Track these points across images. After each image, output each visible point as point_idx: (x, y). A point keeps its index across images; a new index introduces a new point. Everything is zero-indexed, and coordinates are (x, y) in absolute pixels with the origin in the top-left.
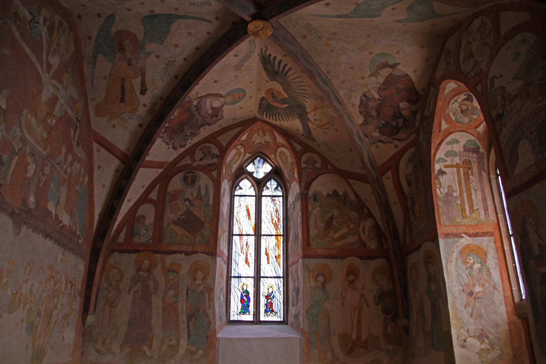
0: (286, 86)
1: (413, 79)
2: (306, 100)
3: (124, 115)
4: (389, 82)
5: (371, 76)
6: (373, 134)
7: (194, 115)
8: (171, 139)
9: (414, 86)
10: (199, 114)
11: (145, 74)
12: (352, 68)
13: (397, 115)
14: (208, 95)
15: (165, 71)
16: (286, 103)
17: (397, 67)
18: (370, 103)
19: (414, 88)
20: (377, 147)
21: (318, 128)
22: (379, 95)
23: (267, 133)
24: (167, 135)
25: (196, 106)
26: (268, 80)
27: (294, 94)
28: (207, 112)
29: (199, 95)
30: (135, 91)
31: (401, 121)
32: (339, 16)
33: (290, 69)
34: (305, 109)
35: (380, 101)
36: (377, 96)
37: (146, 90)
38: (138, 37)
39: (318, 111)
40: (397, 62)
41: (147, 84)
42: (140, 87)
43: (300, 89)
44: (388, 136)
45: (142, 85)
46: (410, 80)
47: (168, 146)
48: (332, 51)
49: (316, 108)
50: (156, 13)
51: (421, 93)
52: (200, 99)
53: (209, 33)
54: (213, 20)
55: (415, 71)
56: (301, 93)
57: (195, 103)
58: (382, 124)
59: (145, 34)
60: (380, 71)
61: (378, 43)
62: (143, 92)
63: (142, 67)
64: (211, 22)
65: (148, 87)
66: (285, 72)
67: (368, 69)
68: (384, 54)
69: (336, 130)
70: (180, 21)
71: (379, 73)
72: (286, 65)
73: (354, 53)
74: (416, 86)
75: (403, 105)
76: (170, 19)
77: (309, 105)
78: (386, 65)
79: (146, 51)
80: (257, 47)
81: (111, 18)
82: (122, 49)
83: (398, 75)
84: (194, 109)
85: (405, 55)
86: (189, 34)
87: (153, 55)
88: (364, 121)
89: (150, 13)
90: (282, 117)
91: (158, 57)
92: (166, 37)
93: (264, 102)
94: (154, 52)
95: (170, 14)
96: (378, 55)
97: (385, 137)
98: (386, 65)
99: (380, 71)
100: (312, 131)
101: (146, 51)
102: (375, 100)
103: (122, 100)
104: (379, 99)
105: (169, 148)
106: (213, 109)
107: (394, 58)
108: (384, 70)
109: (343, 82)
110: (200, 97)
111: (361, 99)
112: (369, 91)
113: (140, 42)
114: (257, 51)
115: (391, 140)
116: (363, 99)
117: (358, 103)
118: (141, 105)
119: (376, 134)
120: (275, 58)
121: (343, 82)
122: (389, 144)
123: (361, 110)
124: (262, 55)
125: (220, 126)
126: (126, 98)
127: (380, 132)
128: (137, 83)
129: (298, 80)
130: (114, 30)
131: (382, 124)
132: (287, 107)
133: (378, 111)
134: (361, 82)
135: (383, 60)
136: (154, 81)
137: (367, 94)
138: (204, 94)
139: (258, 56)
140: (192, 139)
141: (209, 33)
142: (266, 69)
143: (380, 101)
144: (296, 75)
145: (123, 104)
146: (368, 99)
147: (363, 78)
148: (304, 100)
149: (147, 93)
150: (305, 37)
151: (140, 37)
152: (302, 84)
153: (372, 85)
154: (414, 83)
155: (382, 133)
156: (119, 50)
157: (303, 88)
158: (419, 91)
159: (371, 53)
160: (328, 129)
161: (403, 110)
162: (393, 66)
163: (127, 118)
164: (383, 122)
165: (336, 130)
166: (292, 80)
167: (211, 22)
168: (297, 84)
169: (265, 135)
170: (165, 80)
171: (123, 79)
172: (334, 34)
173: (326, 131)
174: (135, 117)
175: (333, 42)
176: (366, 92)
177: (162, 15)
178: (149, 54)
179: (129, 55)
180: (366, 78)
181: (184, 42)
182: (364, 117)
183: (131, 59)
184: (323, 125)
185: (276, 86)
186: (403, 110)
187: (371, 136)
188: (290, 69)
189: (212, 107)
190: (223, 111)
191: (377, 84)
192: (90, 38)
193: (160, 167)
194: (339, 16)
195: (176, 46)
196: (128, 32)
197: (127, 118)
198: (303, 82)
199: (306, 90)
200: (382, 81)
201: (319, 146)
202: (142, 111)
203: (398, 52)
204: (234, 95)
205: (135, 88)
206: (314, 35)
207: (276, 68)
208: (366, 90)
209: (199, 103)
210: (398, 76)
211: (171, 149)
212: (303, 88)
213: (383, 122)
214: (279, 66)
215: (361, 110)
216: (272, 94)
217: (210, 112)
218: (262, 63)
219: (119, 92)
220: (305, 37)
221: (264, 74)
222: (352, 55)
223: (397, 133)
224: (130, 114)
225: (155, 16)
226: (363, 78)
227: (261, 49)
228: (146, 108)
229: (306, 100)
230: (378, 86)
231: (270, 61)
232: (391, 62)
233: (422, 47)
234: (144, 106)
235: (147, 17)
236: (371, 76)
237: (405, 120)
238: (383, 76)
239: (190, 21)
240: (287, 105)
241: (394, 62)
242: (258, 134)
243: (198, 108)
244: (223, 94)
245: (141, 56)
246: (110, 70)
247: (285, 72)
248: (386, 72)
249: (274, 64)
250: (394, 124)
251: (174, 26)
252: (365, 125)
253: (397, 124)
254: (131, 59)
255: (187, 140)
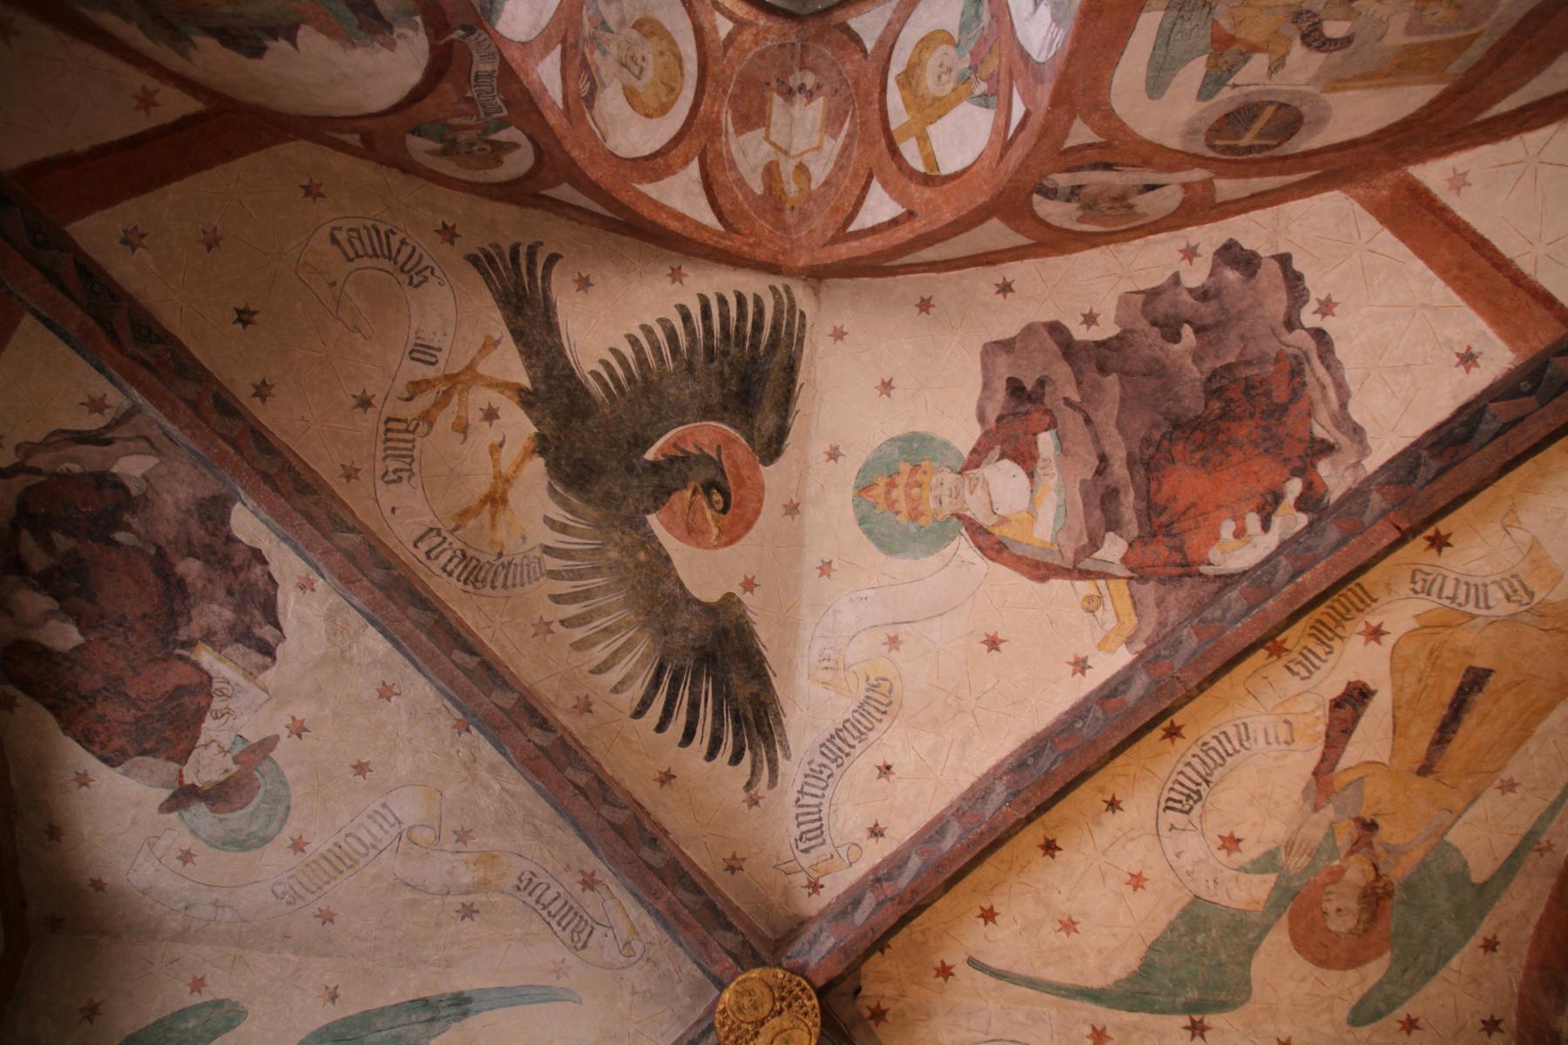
0: (656, 592)
1: (77, 747)
2: (553, 539)
3: (1501, 608)
4: (174, 724)
5: (267, 744)
6: (150, 462)
7: (1131, 462)
8: (1296, 368)
9: (58, 716)
10: (1103, 459)
11: (1315, 773)
12: (361, 768)
13: (70, 586)
14: (1041, 570)
15: (1218, 772)
16: (655, 466)
17: (165, 794)
18: (228, 614)
19: (50, 708)
20: (97, 406)
21: (471, 367)
22: (197, 666)
23: (757, 187)
24: (1310, 414)
25: (1113, 524)
26: (746, 598)
27: (614, 554)
28: (1063, 449)
29: (1085, 587)
30: (1396, 707)
31: (39, 560)
32: (461, 1004)
33: (639, 713)
34: (554, 467)
35: (183, 635)
36: (206, 657)
37: (1337, 704)
38: (1287, 939)
39: (481, 484)
40: (174, 815)
41: (1322, 728)
42: (1363, 721)
43: (587, 595)
44: (67, 477)
45: (1347, 732)
46: (86, 741)
47: (1329, 325)
48: (462, 836)
49: (496, 500)
50: (1184, 1020)
51: (11, 690)
52: (1086, 564)
53: (989, 915)
54: (961, 969)
55: (83, 780)
56: (579, 575)
57: (1113, 549)
58: (128, 528)
59: (1252, 949)
60: (234, 768)
61: (279, 890)
62: (1356, 697)
63: (1316, 808)
64: (972, 962)
65: (1323, 714)
66: (666, 679)
67: (289, 774)
68: (240, 843)
69: (365, 403)
70: (1096, 982)
71: (236, 760)
72: (661, 727)
73: (368, 839)
74: (49, 716)
75: (66, 636)
76: (1134, 994)
77: (536, 509)
78: (220, 795)
79: (1272, 878)
80: (793, 795)
81: (1363, 1014)
82: (1375, 898)
83: (149, 760)
84: (1128, 505)
85: (151, 846)
86: (1069, 926)
87: (1251, 851)
88: (225, 520)
89: (1211, 1019)
90: (675, 350)
91: (1231, 843)
92: (1172, 927)
93: (768, 422)
94: (1242, 869)
95: (1130, 1010)
96: (265, 840)
97: (76, 468)
98: (220, 795)
99: (234, 768)
100: (500, 330)
101: (1272, 878)
102: (208, 637)
103: (1475, 680)
104: (190, 644)
105: (1326, 307)
106: (1026, 458)
107: (194, 832)
108: (216, 777)
109: (386, 692)
110: (1086, 575)
111: (277, 626)
112: (250, 675)
113: (1284, 919)
114: (792, 770)
115: (41, 460)
116: (267, 632)
117: (290, 603)
118: (1388, 641)
119: (132, 467)
120: (711, 754)
121: (386, 692)
122: (38, 436)
123: (258, 570)
124: (770, 747)
125: (1005, 288)
126: (1451, 684)
127: (118, 484)
128: (1371, 739)
129: (600, 653)
130: (1375, 970)
131: (128, 528)
132: (648, 443)
133: (175, 590)
134: (303, 711)
135: (236, 819)
136: (1283, 735)
137: (256, 658)
138: (1058, 585)
139: (790, 736)
140: (1176, 279)
141: (989, 915)
142: (755, 666)
143: (183, 635)
144: (614, 676)
145: (1480, 662)
146: (243, 635)
147: (299, 729)
148: (563, 529)
149: (1338, 690)
150: (589, 883)
151: (1278, 939)
152: (579, 633)
153: (244, 707)
154: (67, 728)
155: (106, 482)
156: (1389, 894)
157: (573, 610)
158: (22, 699)
159: (298, 846)
160: (417, 388)
161: (48, 614)
162: (183, 797)
163: (1496, 595)
164: (121, 536)
165: (365, 403)
166: (629, 646)
167: (972, 962)
168: (602, 622)
169: (771, 171)
170: (1231, 732)
171: (1425, 770)
172: (468, 912)
173: (422, 372)
174: (1448, 591)
175: (466, 878)
176: (266, 668)
177: (1162, 1012)
178: (1268, 862)
179: (1356, 873)
180: (284, 733)
181: (1105, 889)
182: (231, 539)
183: (1351, 852)
184: (443, 401)
185: (704, 571)
186: (48, 614)
187: (156, 450)
188: (639, 713)
189: (1031, 475)
190: (981, 418)
191: (229, 712)
192: (1490, 945)
193: (1420, 197)
194: (461, 1004)
195: (1137, 881)
196: (1322, 963)
197: (1496, 595)
198: (580, 645)
199: (557, 599)
200: (209, 726)
201: (448, 234)
202: (1400, 613)
203: (186, 857)
204: (914, 515)
205: (1388, 721)
206: (551, 894)
207: (707, 686)
208: (269, 677)
209: (1095, 544)
210: (144, 753)
211: (1317, 285)
212: (573, 610)
213: (121, 536)
214: (694, 706)
215: (258, 570)
216: (724, 511)
217: (1046, 442)
218: (775, 700)
219: (1469, 721)
220: (589, 883)
221: (764, 633)
222: (375, 829)
223: (22, 504)
224: (1470, 608)
225: (1189, 1008)
226: (299, 729)
227: (773, 781)
228: (1374, 622)
229: (553, 539)
230: (217, 704)
231: (737, 719)
232: (200, 813)
233: (98, 885)
234: (1376, 634)
235: (1222, 1007)
236: (267, 744)
237: (18, 566)
238: (214, 748)
239: (1054, 974)
240: (650, 455)
241: (187, 815)
242: (802, 169)
243: (1102, 502)
244: (963, 547)
245: (1304, 861)
246: (1466, 817)
247: (666, 679)
248: (207, 767)
249: (717, 713)
250: (63, 542)
251: (1125, 963)
252: (214, 497)
253: (48, 545)
254: (1351, 852)
255: (1203, 295)
